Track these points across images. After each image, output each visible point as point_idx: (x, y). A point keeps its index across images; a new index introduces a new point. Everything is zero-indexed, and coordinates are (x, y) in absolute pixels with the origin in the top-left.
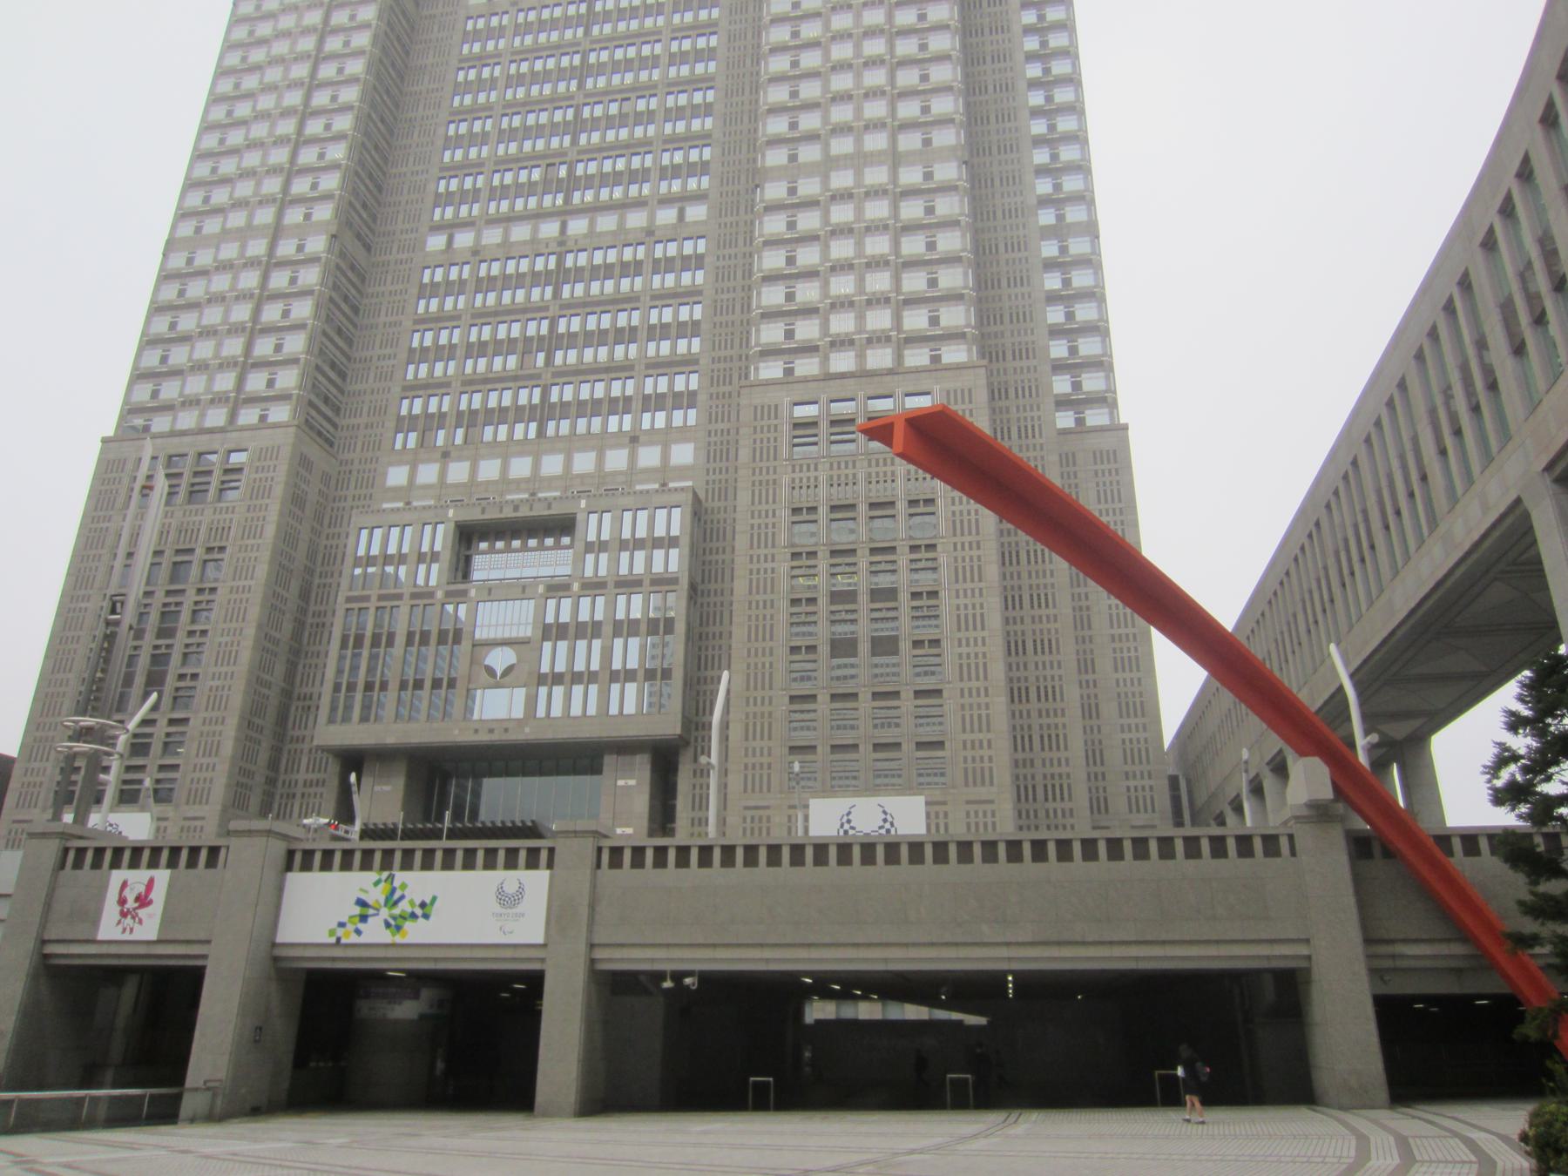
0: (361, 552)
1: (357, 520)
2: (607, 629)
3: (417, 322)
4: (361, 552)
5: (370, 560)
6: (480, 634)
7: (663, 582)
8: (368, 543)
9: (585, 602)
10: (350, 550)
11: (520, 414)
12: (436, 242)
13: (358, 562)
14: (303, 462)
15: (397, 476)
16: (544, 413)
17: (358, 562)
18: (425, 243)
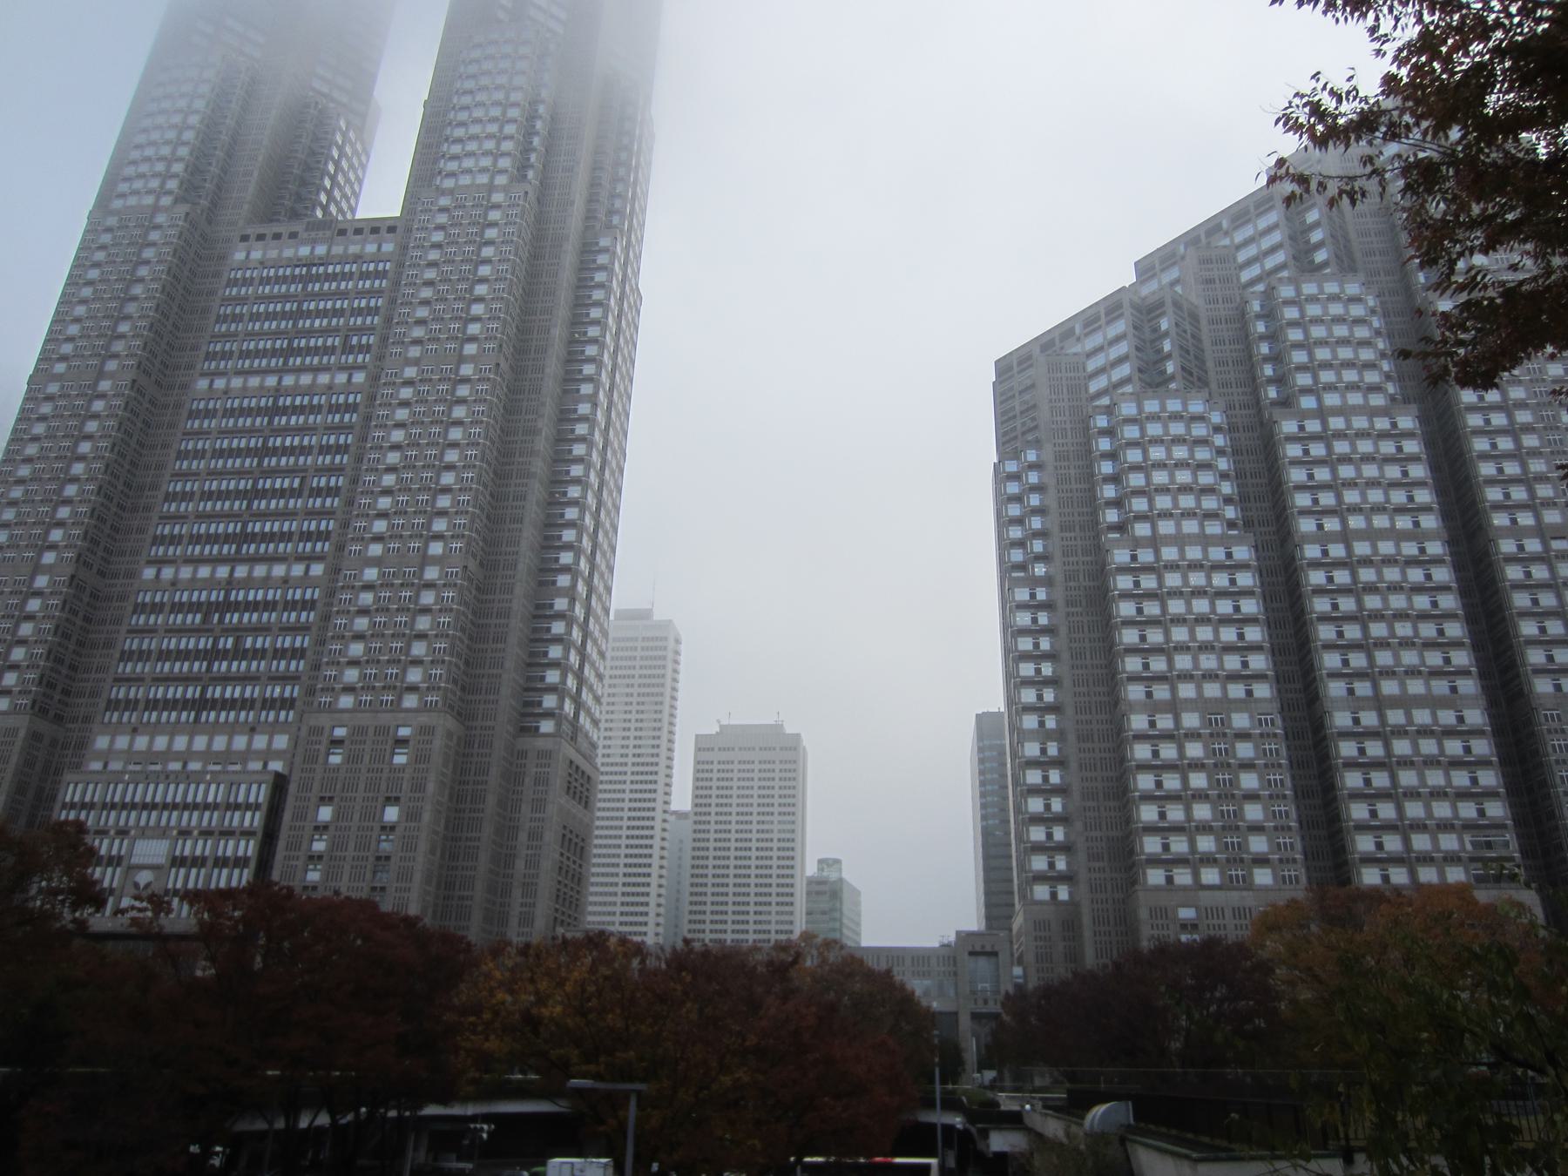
0: (68, 799)
1: (68, 776)
2: (210, 863)
3: (129, 632)
4: (68, 799)
5: (73, 806)
6: (135, 860)
7: (248, 834)
8: (72, 793)
9: (200, 843)
10: (60, 797)
11: (185, 704)
12: (149, 573)
13: (64, 806)
14: (35, 736)
15: (102, 742)
16: (202, 704)
17: (64, 806)
18: (141, 573)
